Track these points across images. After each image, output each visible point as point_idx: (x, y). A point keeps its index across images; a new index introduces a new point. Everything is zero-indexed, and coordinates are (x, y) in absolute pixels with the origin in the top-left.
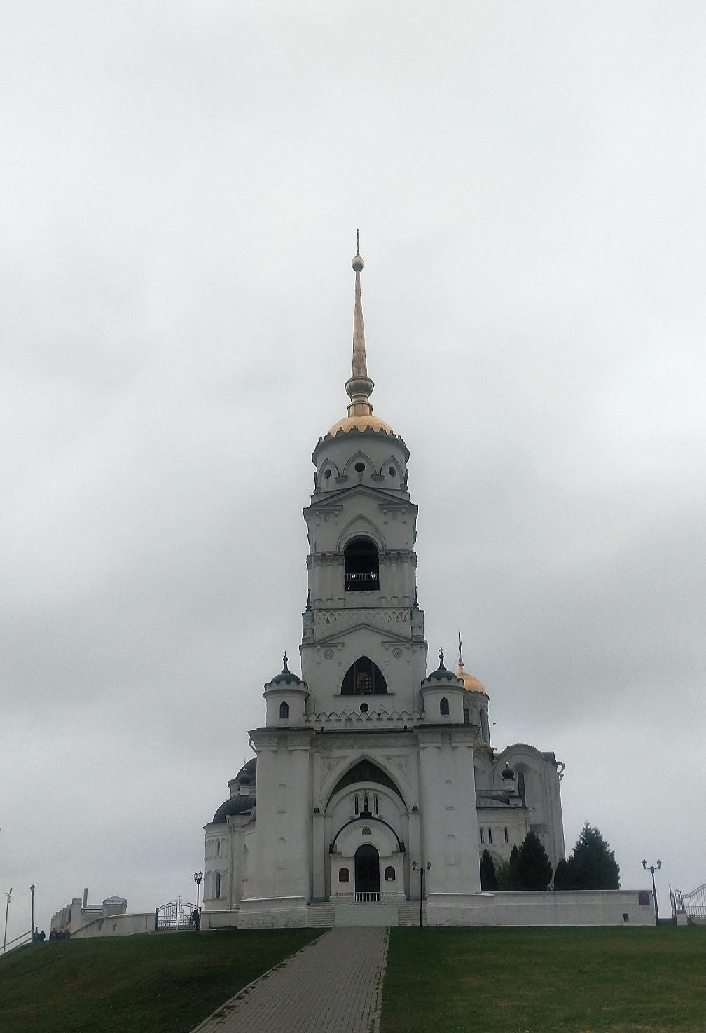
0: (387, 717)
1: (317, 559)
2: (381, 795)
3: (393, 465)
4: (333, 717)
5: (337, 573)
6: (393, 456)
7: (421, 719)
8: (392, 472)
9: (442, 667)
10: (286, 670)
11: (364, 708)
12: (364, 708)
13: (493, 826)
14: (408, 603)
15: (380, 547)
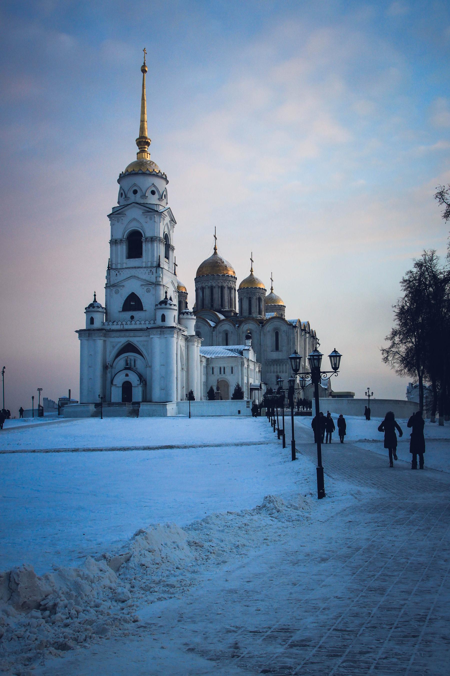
0: (139, 323)
1: (113, 242)
2: (136, 359)
3: (153, 189)
4: (115, 323)
5: (123, 249)
6: (153, 184)
7: (154, 323)
8: (153, 193)
9: (166, 298)
10: (95, 301)
11: (132, 317)
12: (132, 317)
13: (225, 365)
14: (155, 264)
15: (143, 236)
